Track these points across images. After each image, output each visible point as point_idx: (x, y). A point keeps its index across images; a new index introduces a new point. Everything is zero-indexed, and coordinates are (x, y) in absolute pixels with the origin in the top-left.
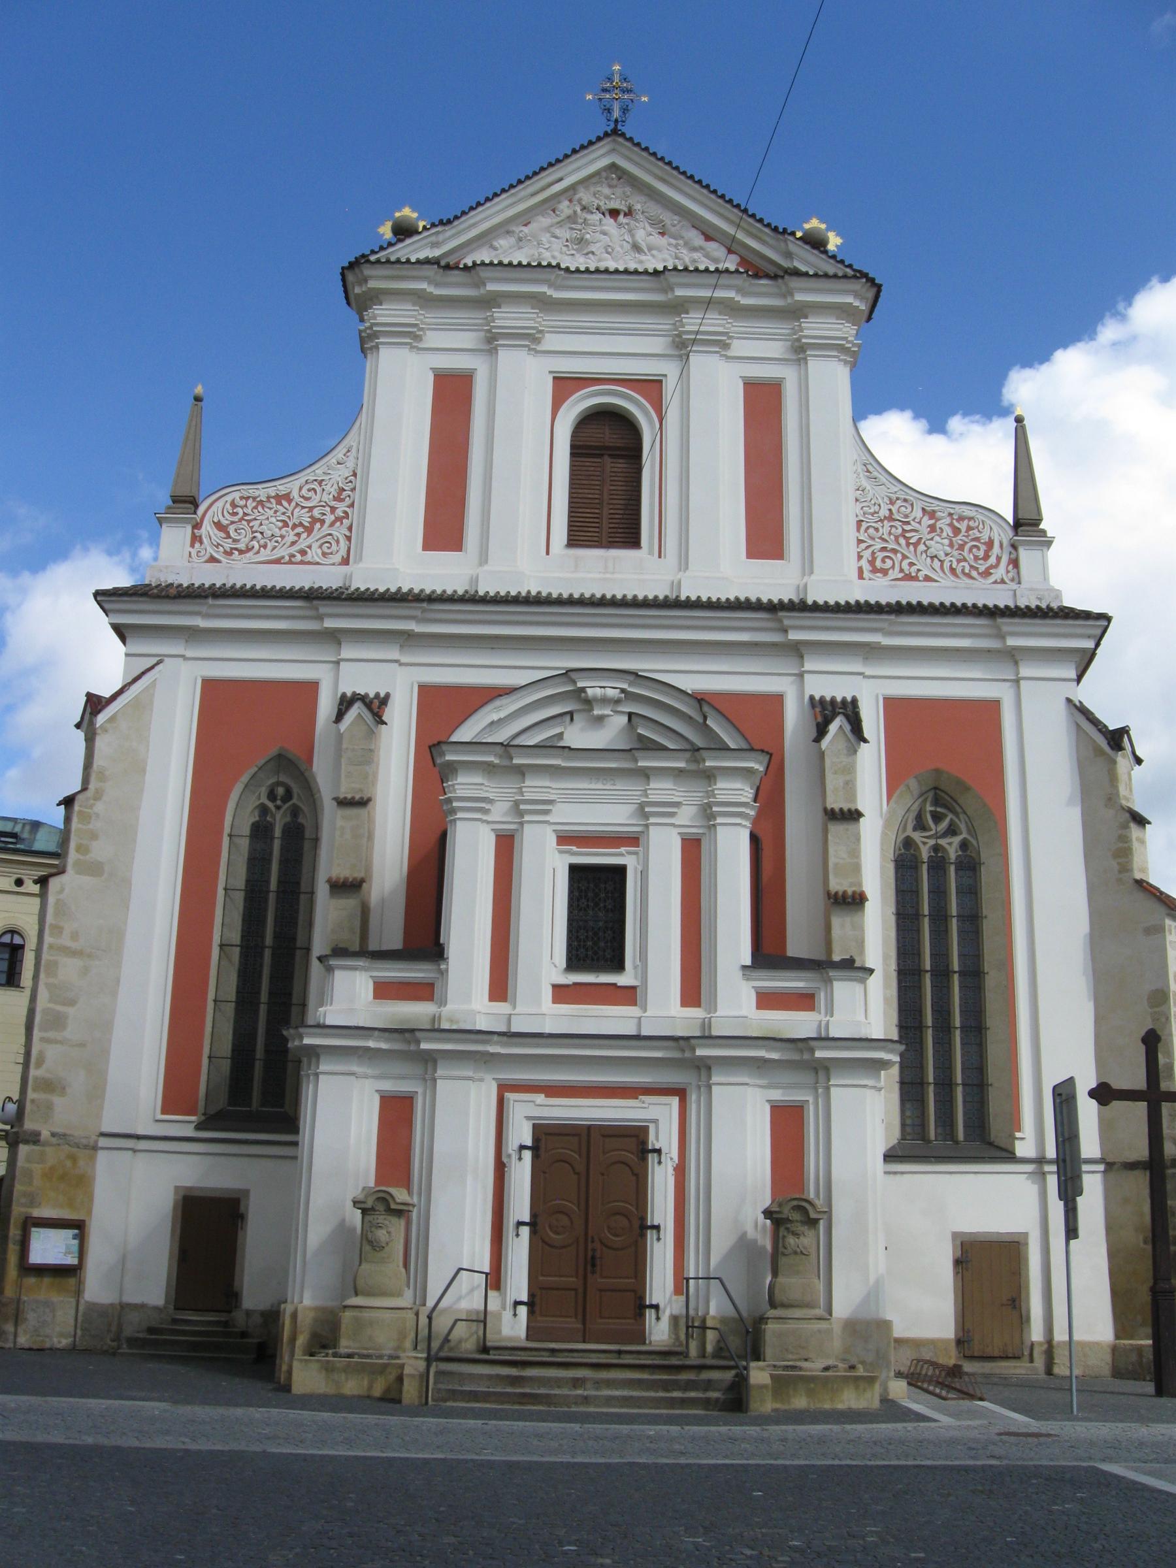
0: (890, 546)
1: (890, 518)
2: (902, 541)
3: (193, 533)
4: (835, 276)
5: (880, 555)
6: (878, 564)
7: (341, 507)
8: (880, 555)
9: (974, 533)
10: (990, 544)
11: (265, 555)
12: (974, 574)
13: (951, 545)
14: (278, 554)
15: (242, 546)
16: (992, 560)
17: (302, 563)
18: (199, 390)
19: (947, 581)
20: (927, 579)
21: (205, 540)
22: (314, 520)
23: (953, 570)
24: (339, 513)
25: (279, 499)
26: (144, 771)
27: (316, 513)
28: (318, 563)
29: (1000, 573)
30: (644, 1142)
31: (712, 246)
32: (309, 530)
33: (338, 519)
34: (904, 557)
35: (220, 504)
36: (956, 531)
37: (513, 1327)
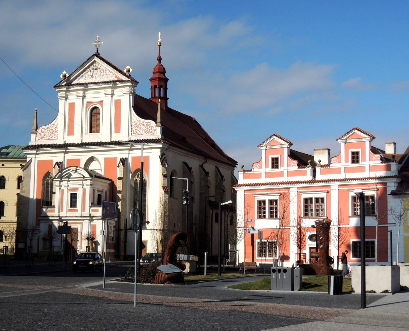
0: (136, 129)
1: (136, 124)
2: (138, 128)
3: (36, 136)
4: (128, 81)
5: (135, 131)
6: (135, 132)
7: (57, 129)
8: (135, 131)
9: (149, 125)
10: (152, 127)
11: (46, 139)
12: (149, 133)
13: (146, 128)
14: (49, 138)
15: (43, 137)
16: (152, 130)
17: (51, 139)
18: (36, 109)
19: (145, 134)
20: (142, 134)
21: (38, 136)
22: (53, 132)
23: (146, 133)
24: (56, 130)
25: (48, 128)
26: (30, 176)
27: (53, 130)
28: (54, 139)
29: (153, 132)
30: (77, 230)
31: (111, 74)
32: (52, 133)
33: (56, 131)
34: (138, 131)
35: (39, 130)
36: (147, 125)
37: (62, 253)
